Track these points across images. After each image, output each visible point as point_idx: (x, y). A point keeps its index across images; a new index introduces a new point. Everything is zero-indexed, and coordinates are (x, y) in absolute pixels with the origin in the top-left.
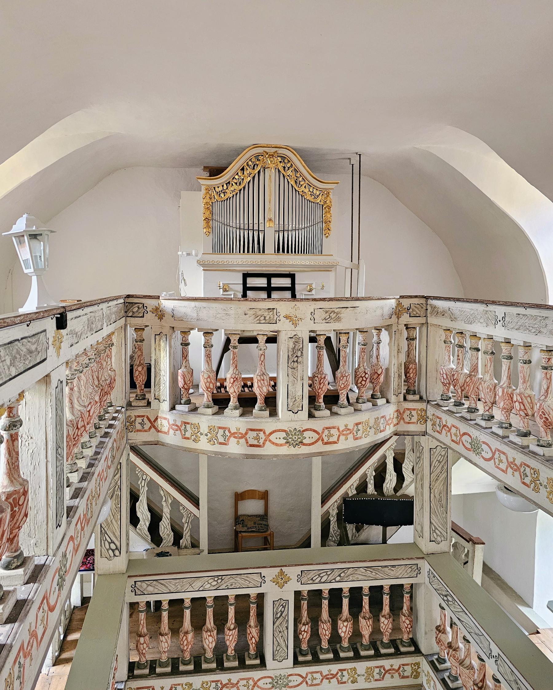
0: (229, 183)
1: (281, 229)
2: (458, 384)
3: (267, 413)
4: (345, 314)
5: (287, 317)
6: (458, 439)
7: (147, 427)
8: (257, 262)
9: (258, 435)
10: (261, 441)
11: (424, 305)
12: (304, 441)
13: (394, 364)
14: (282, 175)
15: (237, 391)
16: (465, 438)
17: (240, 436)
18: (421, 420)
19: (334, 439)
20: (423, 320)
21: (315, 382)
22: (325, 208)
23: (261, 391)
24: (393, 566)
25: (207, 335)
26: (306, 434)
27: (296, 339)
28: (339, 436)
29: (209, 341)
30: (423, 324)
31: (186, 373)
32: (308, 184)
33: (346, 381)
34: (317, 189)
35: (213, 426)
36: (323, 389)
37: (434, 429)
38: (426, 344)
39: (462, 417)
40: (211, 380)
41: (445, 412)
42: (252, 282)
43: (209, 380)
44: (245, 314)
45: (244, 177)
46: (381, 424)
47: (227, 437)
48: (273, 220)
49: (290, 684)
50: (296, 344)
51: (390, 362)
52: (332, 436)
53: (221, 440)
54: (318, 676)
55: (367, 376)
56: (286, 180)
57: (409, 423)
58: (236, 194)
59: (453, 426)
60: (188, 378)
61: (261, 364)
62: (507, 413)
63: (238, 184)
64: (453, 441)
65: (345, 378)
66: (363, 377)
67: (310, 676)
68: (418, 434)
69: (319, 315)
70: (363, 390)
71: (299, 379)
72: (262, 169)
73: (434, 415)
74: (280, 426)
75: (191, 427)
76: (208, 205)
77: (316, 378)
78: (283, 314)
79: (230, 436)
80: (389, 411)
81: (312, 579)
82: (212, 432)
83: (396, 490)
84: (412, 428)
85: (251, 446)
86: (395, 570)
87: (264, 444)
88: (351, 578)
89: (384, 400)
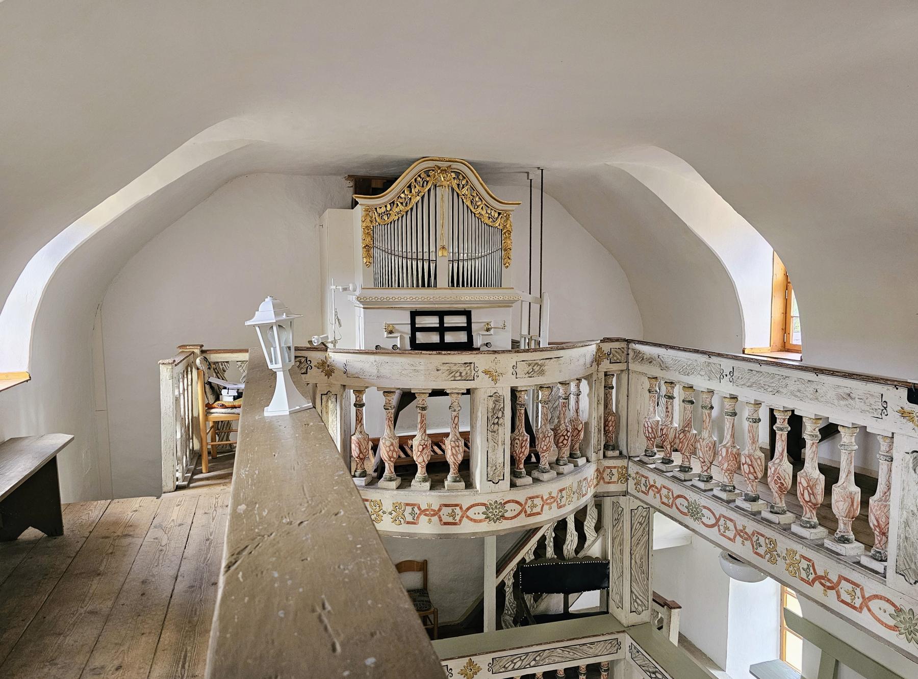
0: (393, 203)
3: (463, 484)
6: (671, 501)
8: (429, 298)
9: (453, 511)
10: (458, 518)
11: (625, 349)
12: (506, 515)
13: (594, 418)
14: (455, 194)
15: (426, 460)
16: (679, 501)
17: (432, 513)
18: (622, 479)
19: (538, 509)
20: (623, 366)
21: (516, 445)
22: (505, 233)
23: (455, 460)
24: (592, 643)
25: (389, 395)
26: (508, 507)
27: (496, 398)
28: (543, 505)
29: (391, 402)
30: (622, 371)
31: (362, 441)
32: (485, 204)
33: (549, 442)
34: (495, 211)
35: (399, 502)
36: (525, 453)
37: (638, 489)
38: (627, 393)
39: (673, 477)
40: (394, 447)
41: (652, 470)
42: (422, 321)
43: (392, 448)
44: (438, 370)
45: (412, 195)
47: (416, 516)
48: (447, 248)
50: (497, 403)
51: (590, 415)
53: (410, 519)
55: (569, 434)
56: (460, 199)
57: (609, 483)
58: (402, 217)
59: (664, 487)
60: (363, 445)
61: (455, 427)
62: (731, 475)
63: (404, 204)
64: (663, 503)
65: (548, 438)
66: (564, 436)
68: (618, 494)
69: (523, 368)
70: (564, 451)
71: (500, 443)
72: (432, 187)
73: (637, 473)
75: (370, 505)
76: (368, 230)
77: (517, 441)
78: (481, 369)
79: (420, 514)
80: (590, 471)
81: (505, 666)
82: (398, 510)
83: (577, 551)
84: (612, 488)
85: (446, 524)
87: (460, 521)
88: (547, 661)
89: (584, 459)
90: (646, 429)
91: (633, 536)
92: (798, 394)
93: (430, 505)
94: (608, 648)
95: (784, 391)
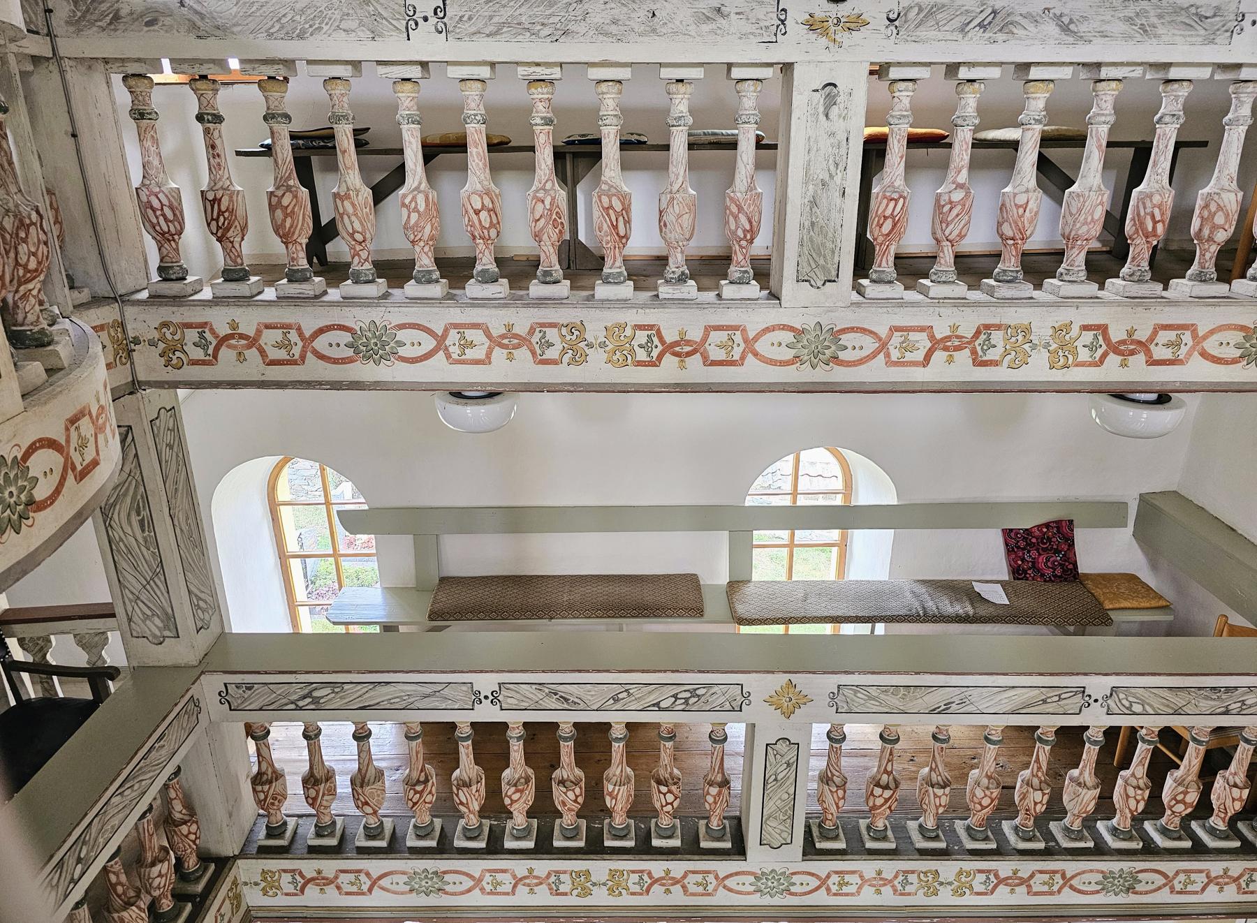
2: (236, 223)
86: (166, 743)
90: (159, 213)
91: (167, 477)
92: (613, 29)
94: (185, 725)
95: (581, 28)
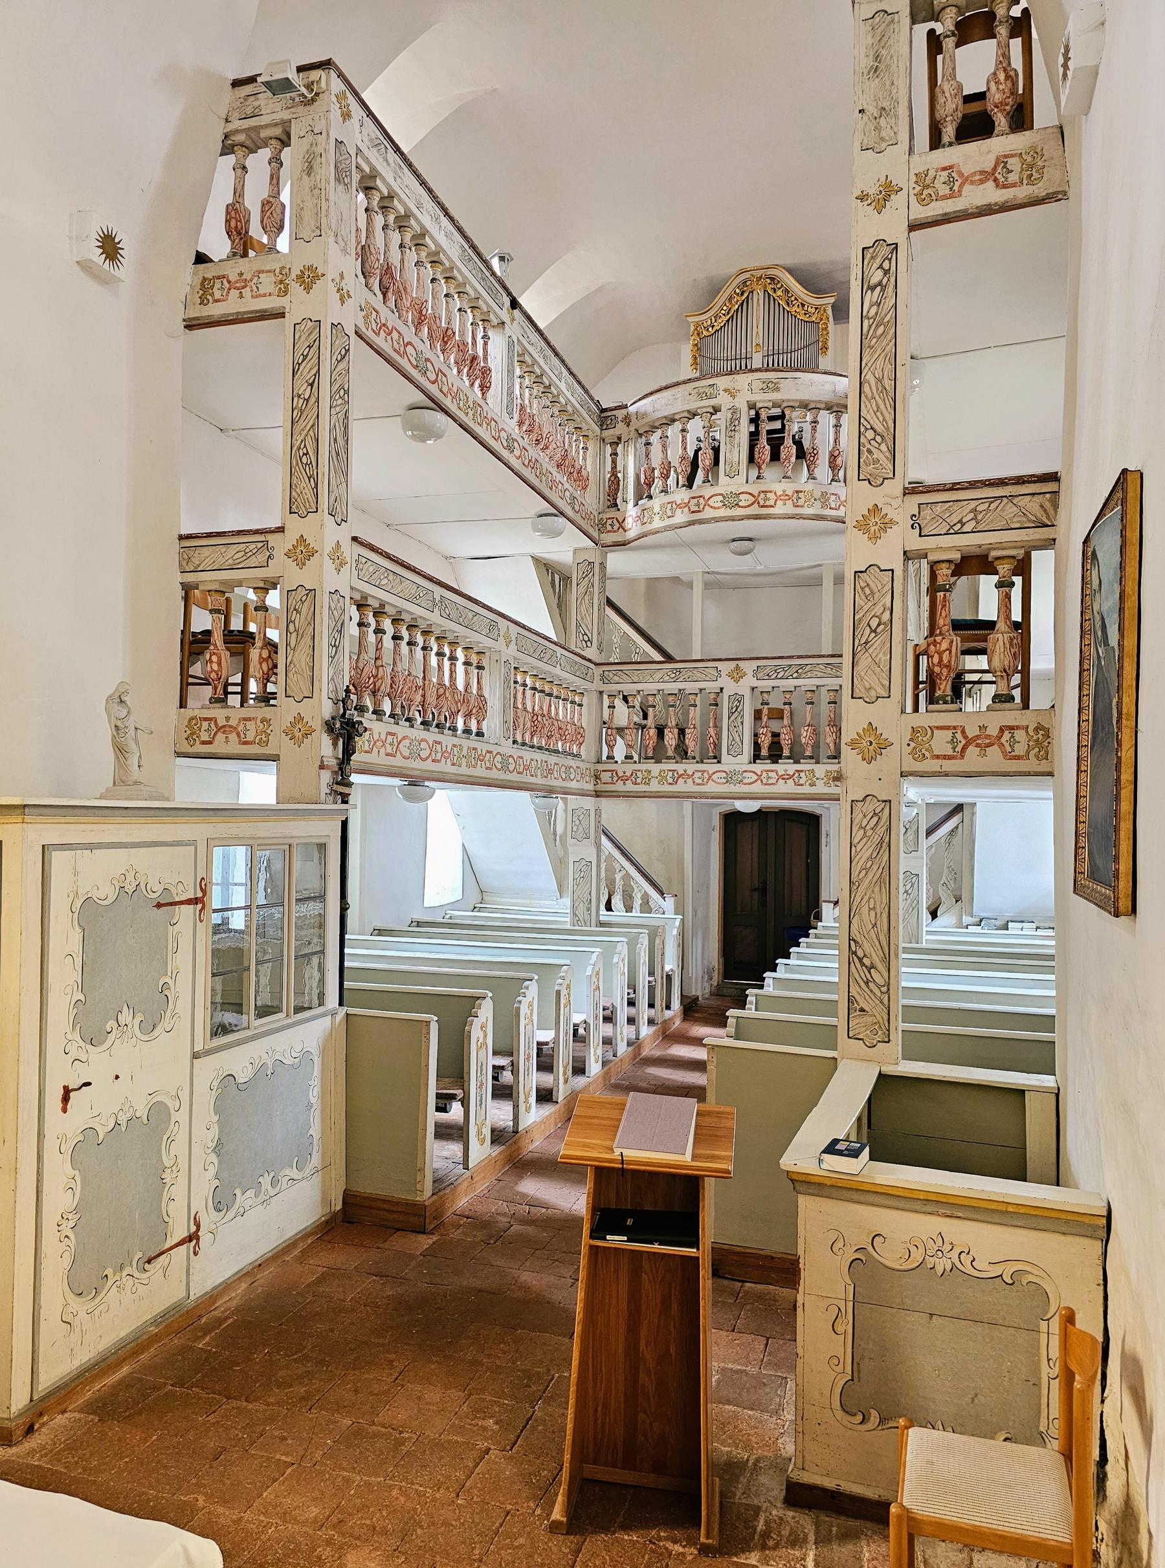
1: (771, 353)
4: (783, 384)
5: (725, 391)
7: (615, 528)
10: (701, 507)
12: (740, 504)
19: (772, 503)
27: (734, 410)
46: (831, 501)
49: (745, 781)
52: (769, 499)
53: (669, 514)
54: (773, 775)
55: (815, 452)
67: (764, 774)
69: (757, 385)
74: (716, 490)
85: (693, 512)
93: (682, 500)
